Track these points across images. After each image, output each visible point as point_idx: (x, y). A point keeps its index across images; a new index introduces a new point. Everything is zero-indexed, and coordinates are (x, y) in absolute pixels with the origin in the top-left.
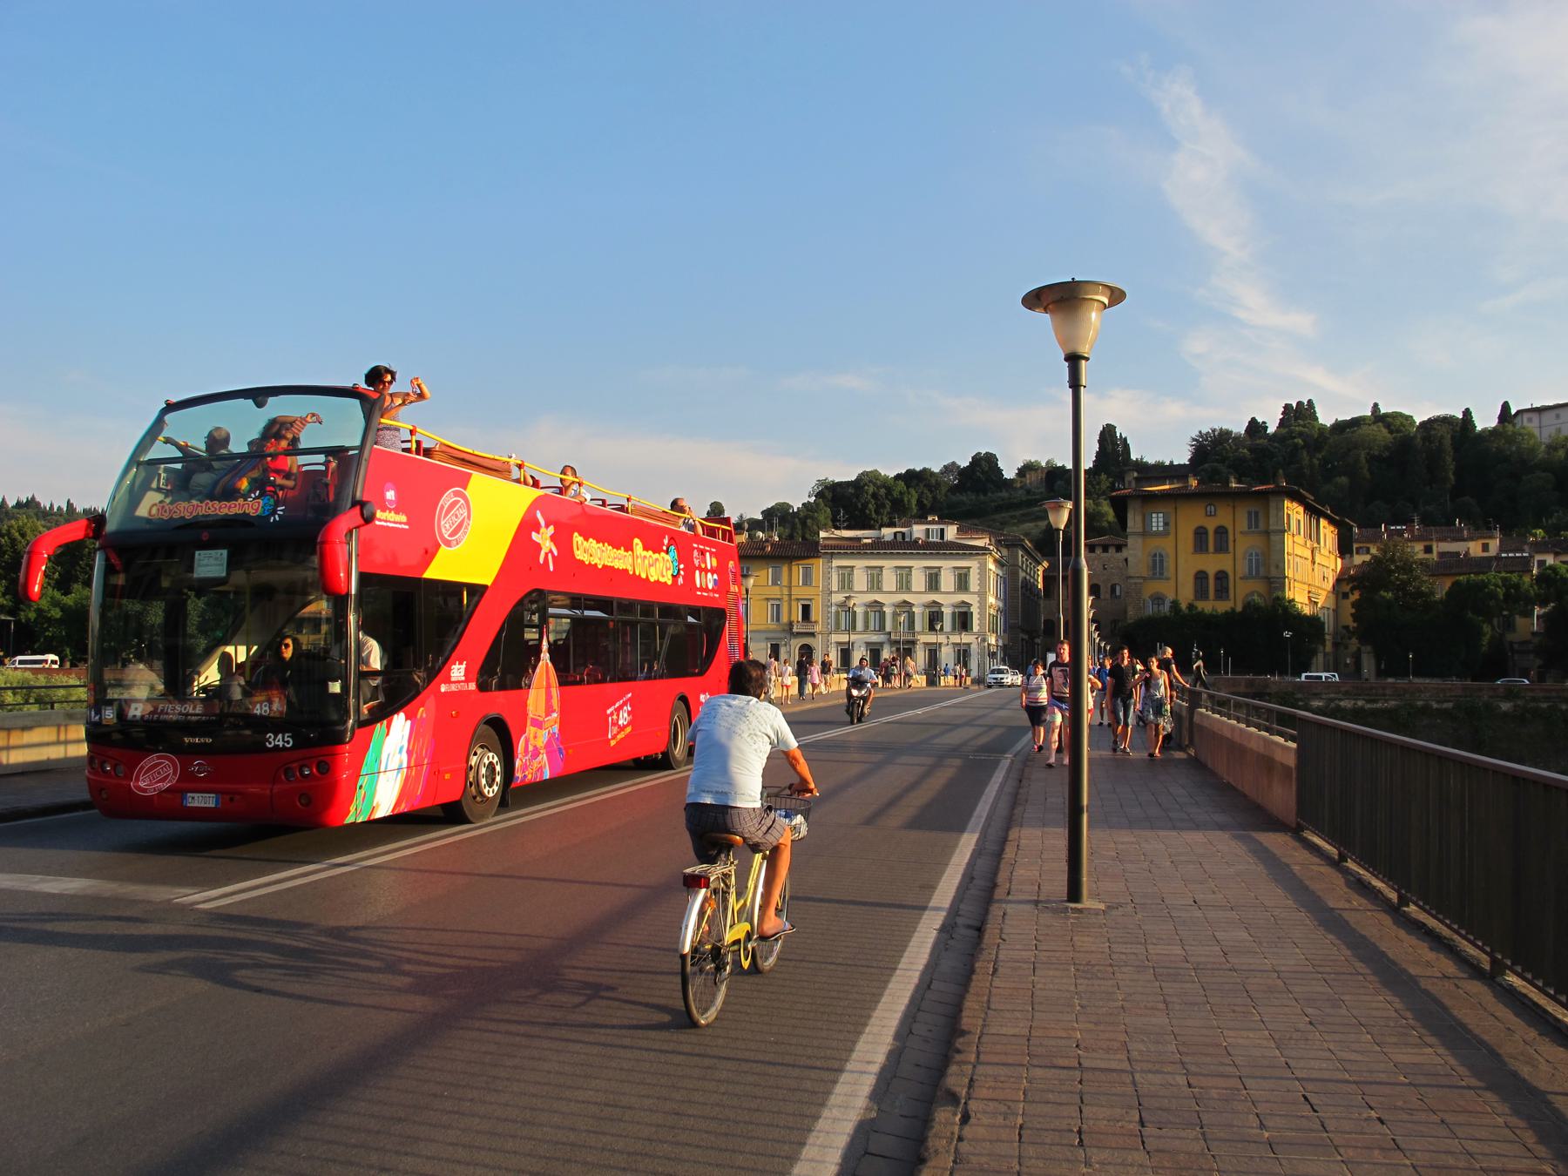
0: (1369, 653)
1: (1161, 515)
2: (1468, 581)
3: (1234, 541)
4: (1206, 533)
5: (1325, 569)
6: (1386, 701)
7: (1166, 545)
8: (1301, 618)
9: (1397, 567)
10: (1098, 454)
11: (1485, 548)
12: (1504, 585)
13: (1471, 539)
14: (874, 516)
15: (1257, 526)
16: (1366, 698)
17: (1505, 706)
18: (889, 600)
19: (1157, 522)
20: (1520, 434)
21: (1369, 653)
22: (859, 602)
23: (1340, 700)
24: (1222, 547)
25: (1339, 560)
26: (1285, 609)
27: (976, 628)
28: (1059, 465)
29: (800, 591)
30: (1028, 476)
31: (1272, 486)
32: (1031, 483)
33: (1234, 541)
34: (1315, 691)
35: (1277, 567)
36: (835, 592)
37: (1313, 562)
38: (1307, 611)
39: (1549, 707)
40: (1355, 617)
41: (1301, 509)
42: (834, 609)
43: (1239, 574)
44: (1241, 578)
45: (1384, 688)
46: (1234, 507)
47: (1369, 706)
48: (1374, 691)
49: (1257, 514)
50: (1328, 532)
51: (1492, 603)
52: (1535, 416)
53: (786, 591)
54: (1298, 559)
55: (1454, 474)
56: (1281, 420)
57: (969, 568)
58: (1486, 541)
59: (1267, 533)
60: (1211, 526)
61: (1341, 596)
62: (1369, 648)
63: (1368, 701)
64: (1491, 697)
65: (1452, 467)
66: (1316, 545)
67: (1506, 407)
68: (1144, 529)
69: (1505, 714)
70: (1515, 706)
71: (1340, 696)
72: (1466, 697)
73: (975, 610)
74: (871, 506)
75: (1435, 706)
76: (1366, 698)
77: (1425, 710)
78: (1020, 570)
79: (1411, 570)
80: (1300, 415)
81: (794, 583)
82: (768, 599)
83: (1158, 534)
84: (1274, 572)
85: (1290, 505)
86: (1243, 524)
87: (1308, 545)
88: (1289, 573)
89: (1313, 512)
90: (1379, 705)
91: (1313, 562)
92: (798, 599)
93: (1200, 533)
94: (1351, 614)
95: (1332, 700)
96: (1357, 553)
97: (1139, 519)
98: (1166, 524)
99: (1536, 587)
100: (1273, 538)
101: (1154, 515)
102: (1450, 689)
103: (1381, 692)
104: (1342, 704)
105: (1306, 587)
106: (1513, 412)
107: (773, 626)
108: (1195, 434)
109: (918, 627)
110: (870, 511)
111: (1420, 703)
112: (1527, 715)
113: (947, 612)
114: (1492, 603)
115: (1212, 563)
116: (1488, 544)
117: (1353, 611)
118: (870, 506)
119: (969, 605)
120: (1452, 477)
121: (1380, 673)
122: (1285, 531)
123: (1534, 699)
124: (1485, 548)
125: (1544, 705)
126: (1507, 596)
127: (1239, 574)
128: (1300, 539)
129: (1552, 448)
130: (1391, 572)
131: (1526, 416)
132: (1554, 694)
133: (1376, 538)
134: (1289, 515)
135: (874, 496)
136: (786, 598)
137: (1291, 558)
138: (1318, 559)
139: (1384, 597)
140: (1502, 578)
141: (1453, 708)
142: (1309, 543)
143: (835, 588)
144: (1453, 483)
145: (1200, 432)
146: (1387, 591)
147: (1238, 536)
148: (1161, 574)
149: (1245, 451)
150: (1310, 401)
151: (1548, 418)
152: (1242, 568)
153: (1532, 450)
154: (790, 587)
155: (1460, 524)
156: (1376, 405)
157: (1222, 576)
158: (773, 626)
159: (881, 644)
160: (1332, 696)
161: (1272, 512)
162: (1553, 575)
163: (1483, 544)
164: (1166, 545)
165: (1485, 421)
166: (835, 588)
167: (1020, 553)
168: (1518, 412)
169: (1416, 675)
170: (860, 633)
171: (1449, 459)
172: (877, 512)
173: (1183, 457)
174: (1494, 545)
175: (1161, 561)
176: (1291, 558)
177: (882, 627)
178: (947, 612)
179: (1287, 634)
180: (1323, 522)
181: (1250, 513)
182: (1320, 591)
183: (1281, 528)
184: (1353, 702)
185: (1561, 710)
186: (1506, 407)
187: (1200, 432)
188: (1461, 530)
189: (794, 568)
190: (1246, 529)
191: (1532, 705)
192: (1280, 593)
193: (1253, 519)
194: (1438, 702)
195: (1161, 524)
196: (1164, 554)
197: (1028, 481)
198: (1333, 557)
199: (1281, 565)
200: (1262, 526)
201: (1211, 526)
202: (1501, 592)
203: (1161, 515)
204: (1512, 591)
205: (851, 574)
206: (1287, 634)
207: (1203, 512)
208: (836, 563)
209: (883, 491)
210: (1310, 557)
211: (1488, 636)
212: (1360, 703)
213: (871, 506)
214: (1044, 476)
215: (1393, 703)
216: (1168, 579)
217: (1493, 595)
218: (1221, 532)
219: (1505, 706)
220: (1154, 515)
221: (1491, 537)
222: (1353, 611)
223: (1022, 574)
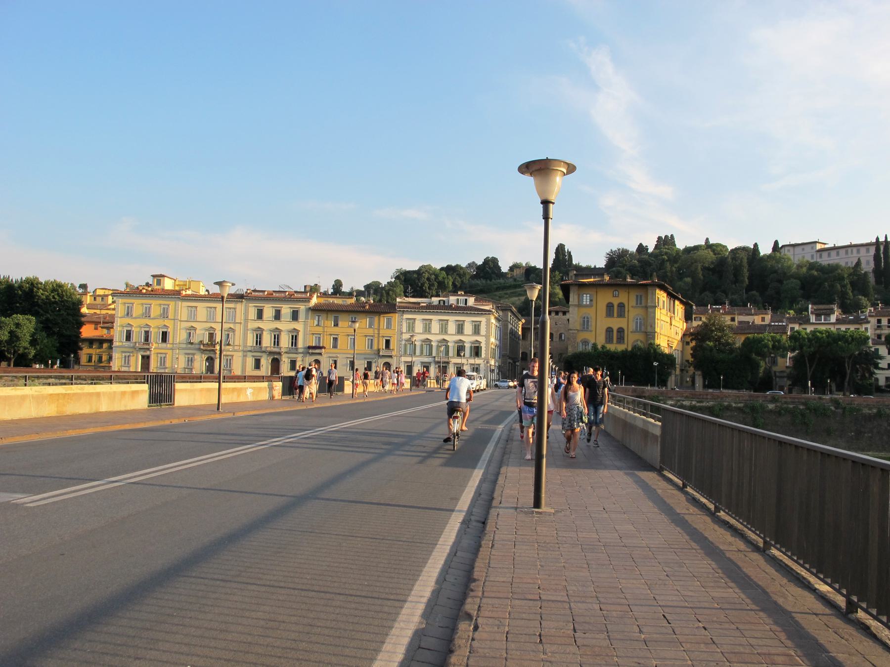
0: (699, 375)
1: (588, 295)
2: (753, 338)
4: (613, 306)
5: (677, 328)
6: (708, 402)
7: (591, 312)
8: (663, 355)
9: (716, 328)
10: (554, 260)
11: (763, 319)
12: (773, 340)
13: (756, 314)
14: (428, 290)
15: (641, 304)
16: (698, 400)
17: (771, 406)
18: (435, 338)
19: (586, 299)
20: (783, 258)
21: (699, 375)
22: (418, 339)
23: (683, 401)
24: (621, 314)
25: (685, 324)
26: (655, 350)
27: (483, 355)
28: (533, 265)
29: (384, 332)
30: (515, 271)
31: (650, 282)
34: (670, 396)
35: (651, 326)
36: (404, 333)
37: (671, 325)
38: (667, 351)
39: (794, 407)
40: (693, 355)
41: (665, 295)
42: (403, 342)
43: (630, 330)
44: (631, 332)
45: (707, 395)
46: (629, 293)
47: (698, 404)
48: (701, 396)
49: (641, 296)
50: (679, 308)
51: (766, 350)
52: (791, 249)
53: (376, 332)
54: (662, 322)
55: (748, 279)
57: (480, 322)
58: (763, 316)
59: (646, 307)
60: (616, 302)
61: (685, 343)
62: (699, 373)
63: (698, 402)
64: (764, 401)
65: (747, 274)
66: (672, 315)
67: (776, 243)
68: (579, 302)
69: (771, 411)
70: (776, 406)
71: (683, 399)
72: (750, 401)
73: (483, 345)
74: (427, 285)
75: (734, 405)
76: (698, 400)
77: (728, 408)
79: (724, 330)
80: (665, 242)
81: (381, 327)
82: (366, 336)
83: (586, 306)
84: (649, 329)
85: (659, 292)
86: (633, 302)
87: (668, 315)
88: (657, 330)
89: (671, 296)
90: (704, 404)
91: (671, 325)
92: (383, 337)
93: (610, 306)
94: (691, 354)
95: (679, 401)
96: (695, 320)
97: (576, 297)
98: (591, 300)
99: (789, 342)
100: (649, 310)
101: (585, 295)
102: (742, 396)
103: (705, 397)
104: (684, 403)
105: (667, 338)
106: (780, 246)
107: (369, 351)
108: (608, 251)
109: (451, 354)
110: (426, 287)
111: (726, 404)
112: (782, 411)
113: (467, 346)
114: (766, 350)
115: (616, 323)
116: (764, 318)
117: (692, 352)
118: (426, 285)
119: (480, 343)
120: (747, 280)
121: (705, 386)
122: (656, 307)
123: (786, 403)
124: (763, 319)
125: (791, 406)
126: (774, 346)
127: (630, 330)
128: (664, 311)
129: (799, 266)
130: (713, 331)
131: (787, 248)
132: (797, 400)
133: (705, 312)
134: (658, 298)
135: (428, 279)
136: (376, 335)
137: (659, 321)
138: (673, 323)
139: (708, 345)
140: (771, 336)
141: (743, 407)
142: (669, 313)
143: (404, 331)
144: (747, 283)
146: (710, 341)
147: (631, 309)
148: (588, 328)
149: (636, 261)
151: (798, 250)
152: (632, 327)
153: (789, 267)
154: (379, 330)
155: (750, 306)
156: (707, 239)
157: (621, 331)
158: (369, 351)
159: (430, 363)
160: (679, 398)
161: (649, 296)
162: (798, 336)
164: (591, 312)
165: (765, 250)
166: (404, 331)
167: (509, 314)
168: (783, 246)
169: (725, 387)
170: (417, 356)
171: (745, 270)
172: (429, 288)
173: (601, 263)
174: (768, 318)
175: (588, 321)
176: (659, 321)
177: (431, 354)
178: (467, 346)
179: (655, 364)
180: (677, 302)
181: (637, 296)
182: (674, 341)
183: (653, 305)
184: (690, 402)
185: (800, 409)
186: (776, 243)
188: (750, 309)
189: (382, 319)
190: (635, 305)
191: (785, 406)
192: (652, 341)
193: (639, 299)
194: (735, 403)
195: (588, 300)
198: (681, 322)
199: (653, 325)
200: (643, 305)
201: (616, 302)
202: (770, 344)
203: (588, 295)
204: (777, 343)
205: (414, 323)
206: (655, 364)
207: (612, 295)
208: (406, 316)
209: (433, 277)
210: (669, 321)
211: (763, 368)
212: (694, 403)
213: (427, 285)
215: (712, 403)
216: (591, 331)
217: (766, 346)
218: (621, 306)
219: (771, 406)
220: (585, 295)
221: (766, 314)
222: (692, 352)
223: (510, 326)
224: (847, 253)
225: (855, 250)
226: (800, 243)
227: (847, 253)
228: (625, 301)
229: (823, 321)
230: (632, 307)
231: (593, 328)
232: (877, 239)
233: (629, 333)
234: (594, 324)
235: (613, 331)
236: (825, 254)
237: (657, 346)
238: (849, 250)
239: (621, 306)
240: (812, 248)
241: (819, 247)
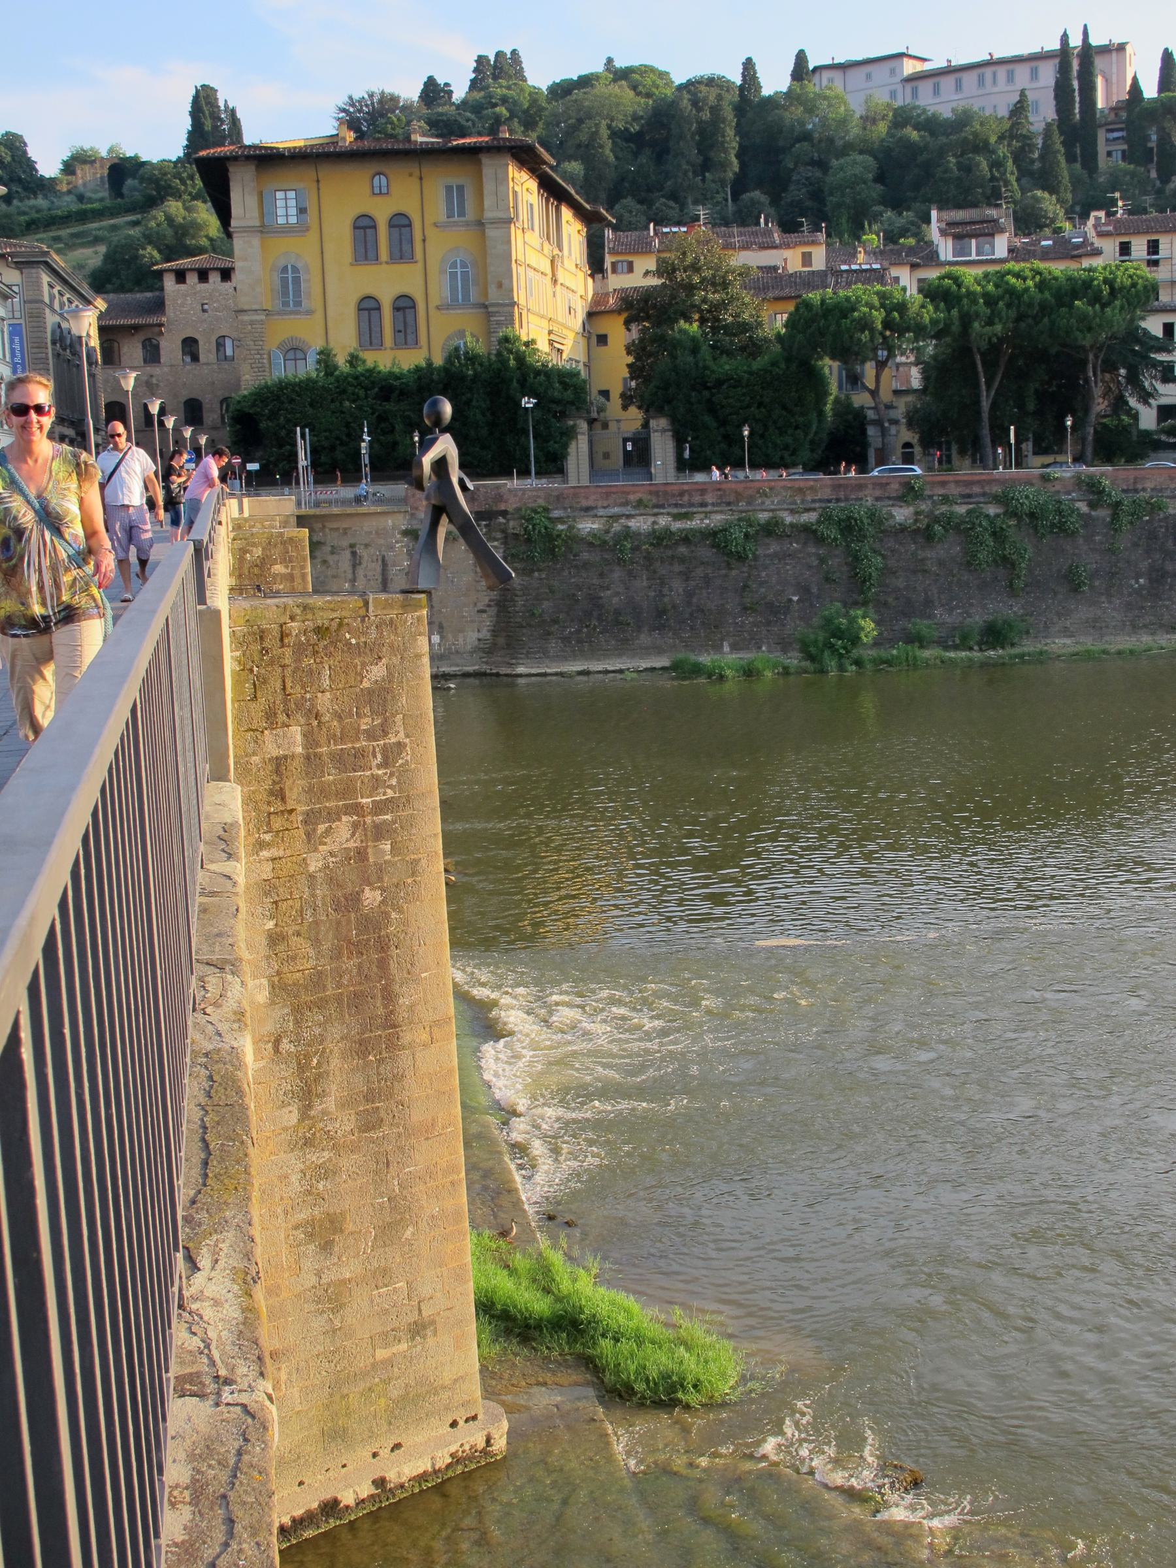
0: (664, 431)
1: (292, 194)
2: (823, 301)
3: (424, 241)
5: (571, 295)
6: (707, 515)
7: (303, 250)
8: (547, 373)
9: (703, 280)
11: (807, 259)
12: (883, 306)
13: (788, 246)
15: (462, 213)
16: (675, 511)
17: (902, 514)
19: (285, 207)
20: (826, 98)
21: (664, 431)
23: (629, 517)
24: (402, 253)
25: (590, 280)
26: (520, 359)
28: (130, 153)
30: (79, 172)
31: (487, 139)
32: (84, 185)
33: (424, 241)
34: (585, 503)
35: (500, 285)
37: (555, 281)
38: (554, 361)
39: (969, 512)
40: (786, 326)
41: (533, 185)
43: (435, 301)
44: (438, 308)
45: (703, 492)
47: (677, 525)
48: (686, 498)
49: (461, 189)
50: (573, 230)
51: (865, 337)
52: (837, 75)
54: (531, 273)
55: (737, 156)
56: (472, 81)
58: (807, 249)
59: (480, 224)
60: (382, 212)
61: (594, 340)
63: (677, 517)
64: (877, 499)
65: (735, 145)
66: (556, 252)
67: (801, 58)
68: (262, 215)
69: (903, 529)
70: (917, 513)
71: (628, 510)
72: (838, 500)
75: (789, 519)
76: (675, 511)
77: (771, 530)
78: (47, 311)
79: (725, 285)
83: (287, 230)
84: (494, 296)
85: (517, 175)
86: (437, 208)
87: (546, 251)
88: (520, 296)
89: (552, 190)
90: (695, 523)
91: (555, 281)
93: (364, 226)
94: (628, 366)
95: (615, 518)
96: (614, 271)
97: (252, 201)
98: (302, 211)
99: (931, 307)
100: (491, 232)
101: (280, 195)
102: (811, 488)
103: (697, 499)
104: (633, 524)
105: (545, 323)
106: (811, 68)
108: (342, 100)
111: (763, 517)
112: (937, 528)
114: (865, 337)
116: (810, 254)
117: (630, 359)
120: (735, 161)
121: (683, 466)
122: (509, 221)
123: (946, 499)
124: (807, 259)
125: (962, 510)
126: (887, 324)
127: (435, 301)
128: (534, 238)
129: (869, 120)
130: (690, 288)
131: (826, 75)
132: (976, 489)
133: (644, 248)
134: (515, 193)
137: (521, 270)
138: (561, 278)
139: (683, 332)
140: (877, 293)
141: (819, 522)
142: (547, 247)
144: (737, 169)
145: (351, 98)
146: (1147, 138)
147: (431, 232)
148: (298, 303)
150: (514, 52)
151: (856, 76)
152: (440, 290)
153: (843, 122)
155: (766, 224)
157: (404, 305)
160: (616, 510)
161: (488, 186)
162: (954, 287)
163: (804, 254)
164: (303, 250)
167: (45, 278)
168: (816, 69)
169: (754, 466)
171: (730, 132)
174: (820, 258)
175: (297, 281)
176: (521, 270)
179: (528, 402)
180: (567, 214)
181: (449, 189)
182: (565, 332)
183: (501, 215)
184: (651, 519)
185: (987, 516)
186: (801, 58)
187: (351, 98)
188: (768, 233)
190: (442, 217)
191: (944, 508)
192: (509, 331)
193: (455, 196)
194: (792, 512)
195: (293, 211)
196: (299, 265)
197: (80, 181)
198: (581, 275)
199: (505, 282)
200: (470, 215)
201: (382, 212)
202: (878, 316)
203: (292, 194)
204: (896, 314)
206: (528, 402)
207: (368, 190)
210: (548, 271)
211: (832, 397)
212: (663, 521)
214: (106, 172)
215: (719, 517)
216: (309, 312)
217: (865, 324)
218: (400, 223)
219: (902, 514)
220: (280, 195)
221: (814, 243)
222: (630, 359)
223: (51, 319)
224: (981, 81)
225: (1002, 71)
226: (859, 58)
227: (981, 81)
228: (410, 207)
229: (974, 257)
230: (436, 225)
231: (316, 303)
232: (1065, 38)
233: (432, 311)
234: (316, 289)
235: (379, 309)
236: (925, 87)
237: (527, 344)
238: (988, 72)
239: (400, 223)
240: (893, 72)
241: (909, 68)
